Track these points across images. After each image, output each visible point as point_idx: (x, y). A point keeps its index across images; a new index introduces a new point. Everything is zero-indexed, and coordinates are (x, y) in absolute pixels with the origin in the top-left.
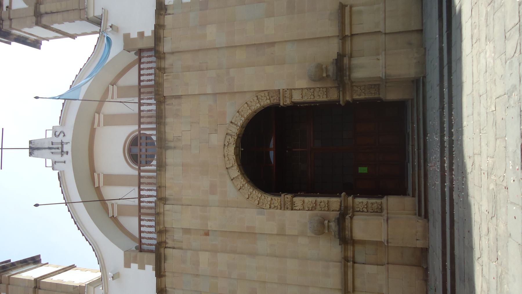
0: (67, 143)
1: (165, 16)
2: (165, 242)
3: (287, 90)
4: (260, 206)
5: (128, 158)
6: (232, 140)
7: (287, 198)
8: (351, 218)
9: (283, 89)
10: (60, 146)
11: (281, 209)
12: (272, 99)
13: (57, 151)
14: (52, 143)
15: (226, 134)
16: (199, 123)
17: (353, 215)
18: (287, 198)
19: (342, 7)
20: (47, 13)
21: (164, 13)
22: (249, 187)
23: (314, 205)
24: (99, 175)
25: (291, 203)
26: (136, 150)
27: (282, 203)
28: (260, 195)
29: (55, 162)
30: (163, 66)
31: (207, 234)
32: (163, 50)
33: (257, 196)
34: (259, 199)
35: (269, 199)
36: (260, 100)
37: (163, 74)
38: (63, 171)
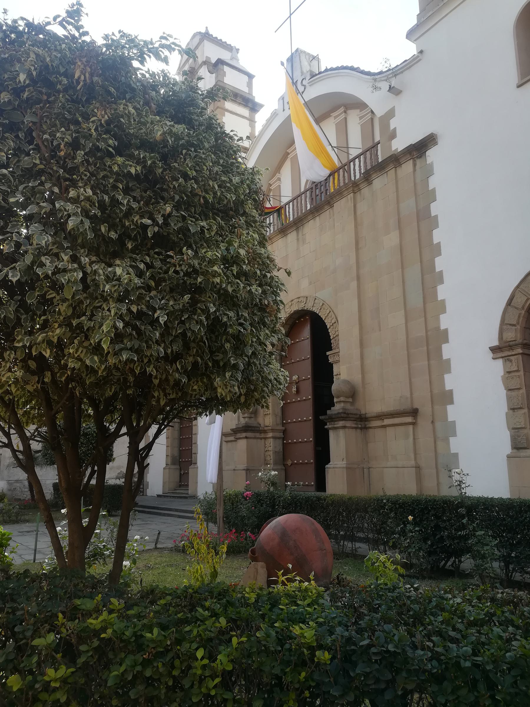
1: (411, 161)
8: (246, 438)
16: (316, 260)
19: (414, 413)
30: (361, 186)
38: (278, 114)
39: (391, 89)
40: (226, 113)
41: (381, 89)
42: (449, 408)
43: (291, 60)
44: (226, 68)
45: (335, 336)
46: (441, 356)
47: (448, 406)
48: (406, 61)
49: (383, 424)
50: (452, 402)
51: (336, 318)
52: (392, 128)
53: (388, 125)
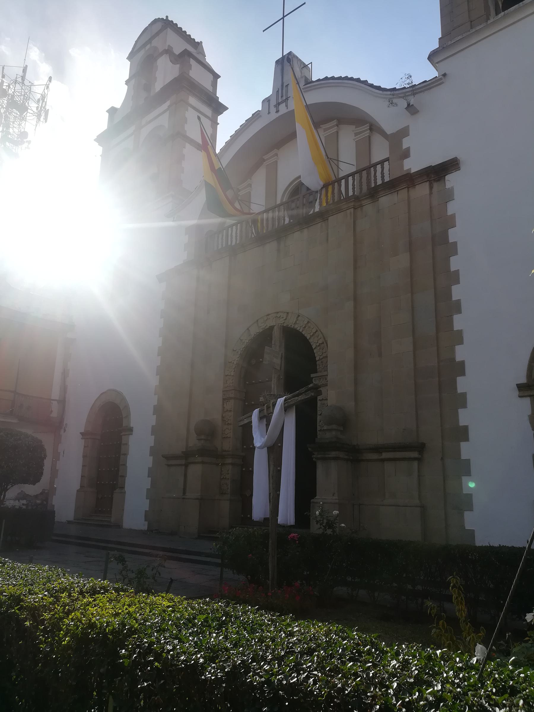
0: (287, 106)
1: (428, 183)
3: (327, 381)
5: (294, 184)
7: (232, 393)
8: (203, 463)
9: (327, 375)
10: (284, 98)
12: (321, 361)
14: (286, 86)
15: (287, 312)
18: (232, 393)
19: (421, 448)
21: (432, 179)
22: (241, 350)
23: (227, 423)
25: (228, 398)
28: (235, 363)
32: (381, 196)
33: (235, 360)
34: (232, 362)
35: (232, 374)
36: (319, 348)
37: (353, 207)
38: (261, 116)
39: (409, 106)
40: (189, 108)
41: (397, 105)
42: (463, 445)
44: (192, 62)
45: (321, 357)
46: (456, 389)
47: (461, 443)
48: (425, 81)
49: (381, 457)
50: (467, 439)
51: (324, 338)
52: (405, 146)
53: (400, 143)
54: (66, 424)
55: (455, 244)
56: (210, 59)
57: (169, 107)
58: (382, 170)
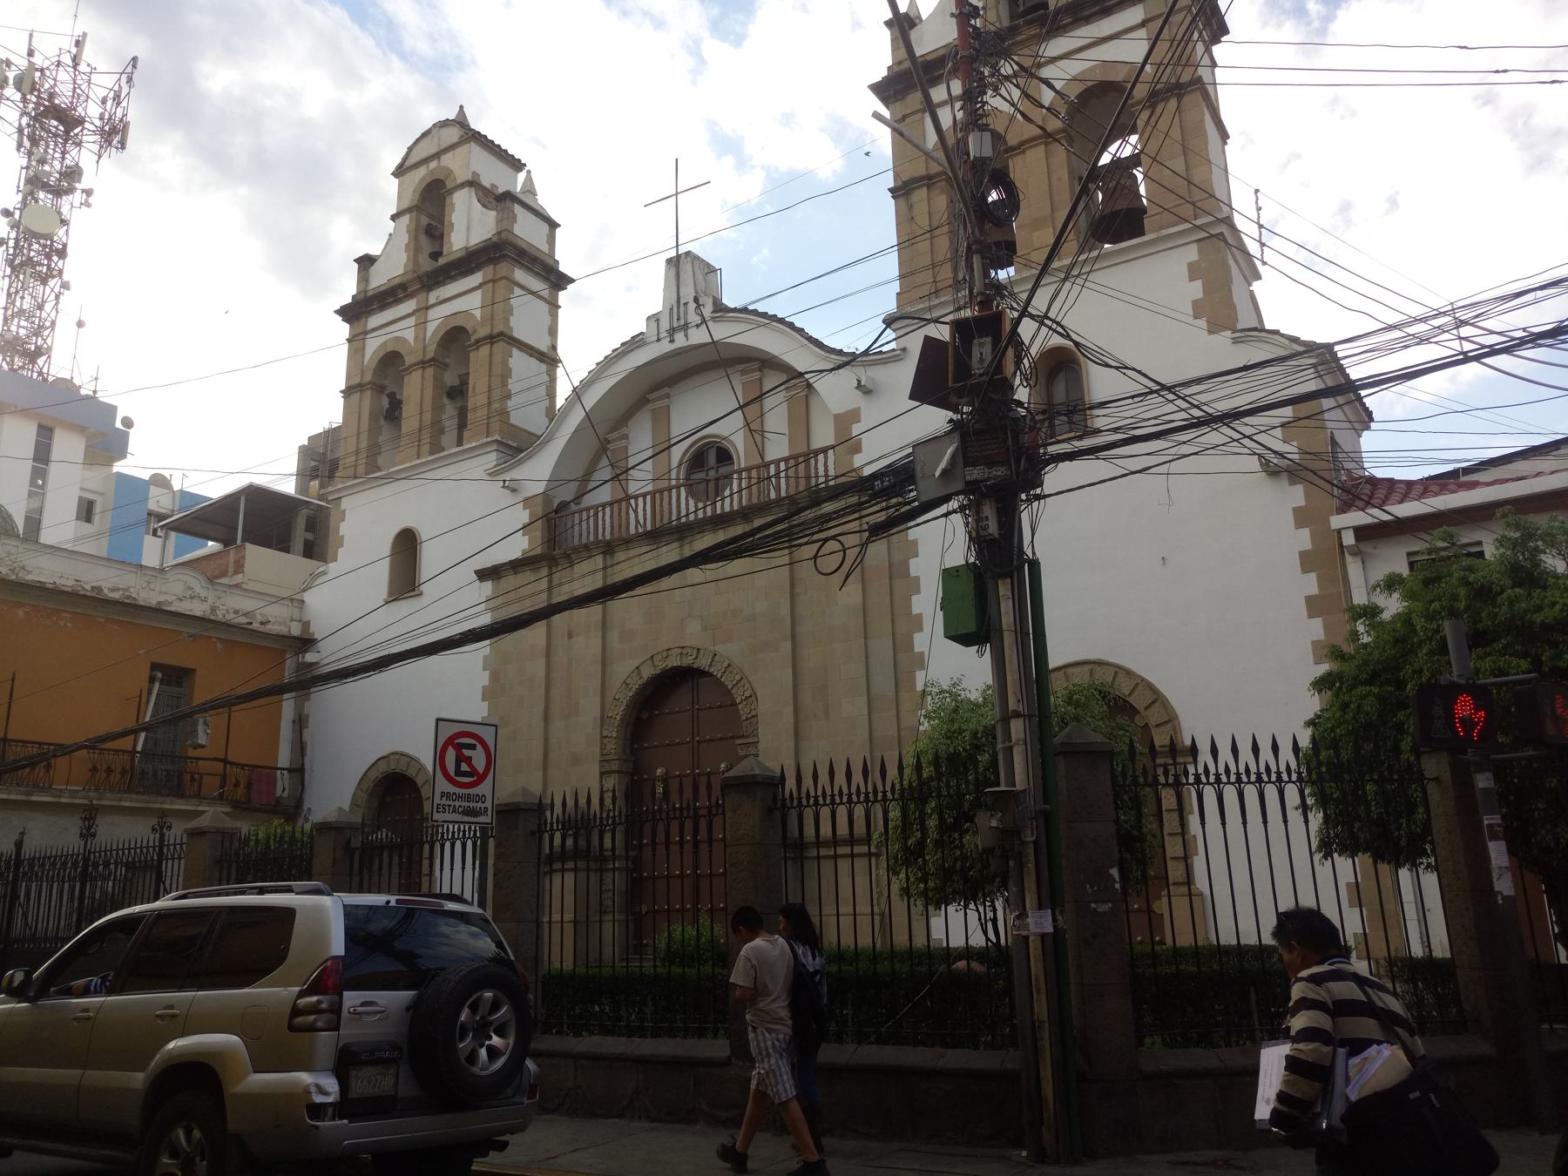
0: (686, 336)
2: (557, 565)
4: (603, 718)
6: (687, 661)
10: (682, 322)
11: (602, 755)
13: (675, 317)
14: (686, 304)
17: (596, 871)
20: (910, 207)
24: (668, 396)
26: (712, 458)
27: (607, 758)
28: (618, 718)
29: (658, 320)
31: (570, 636)
43: (675, 263)
44: (518, 209)
54: (309, 809)
55: (918, 578)
56: (547, 200)
57: (481, 285)
58: (826, 462)
